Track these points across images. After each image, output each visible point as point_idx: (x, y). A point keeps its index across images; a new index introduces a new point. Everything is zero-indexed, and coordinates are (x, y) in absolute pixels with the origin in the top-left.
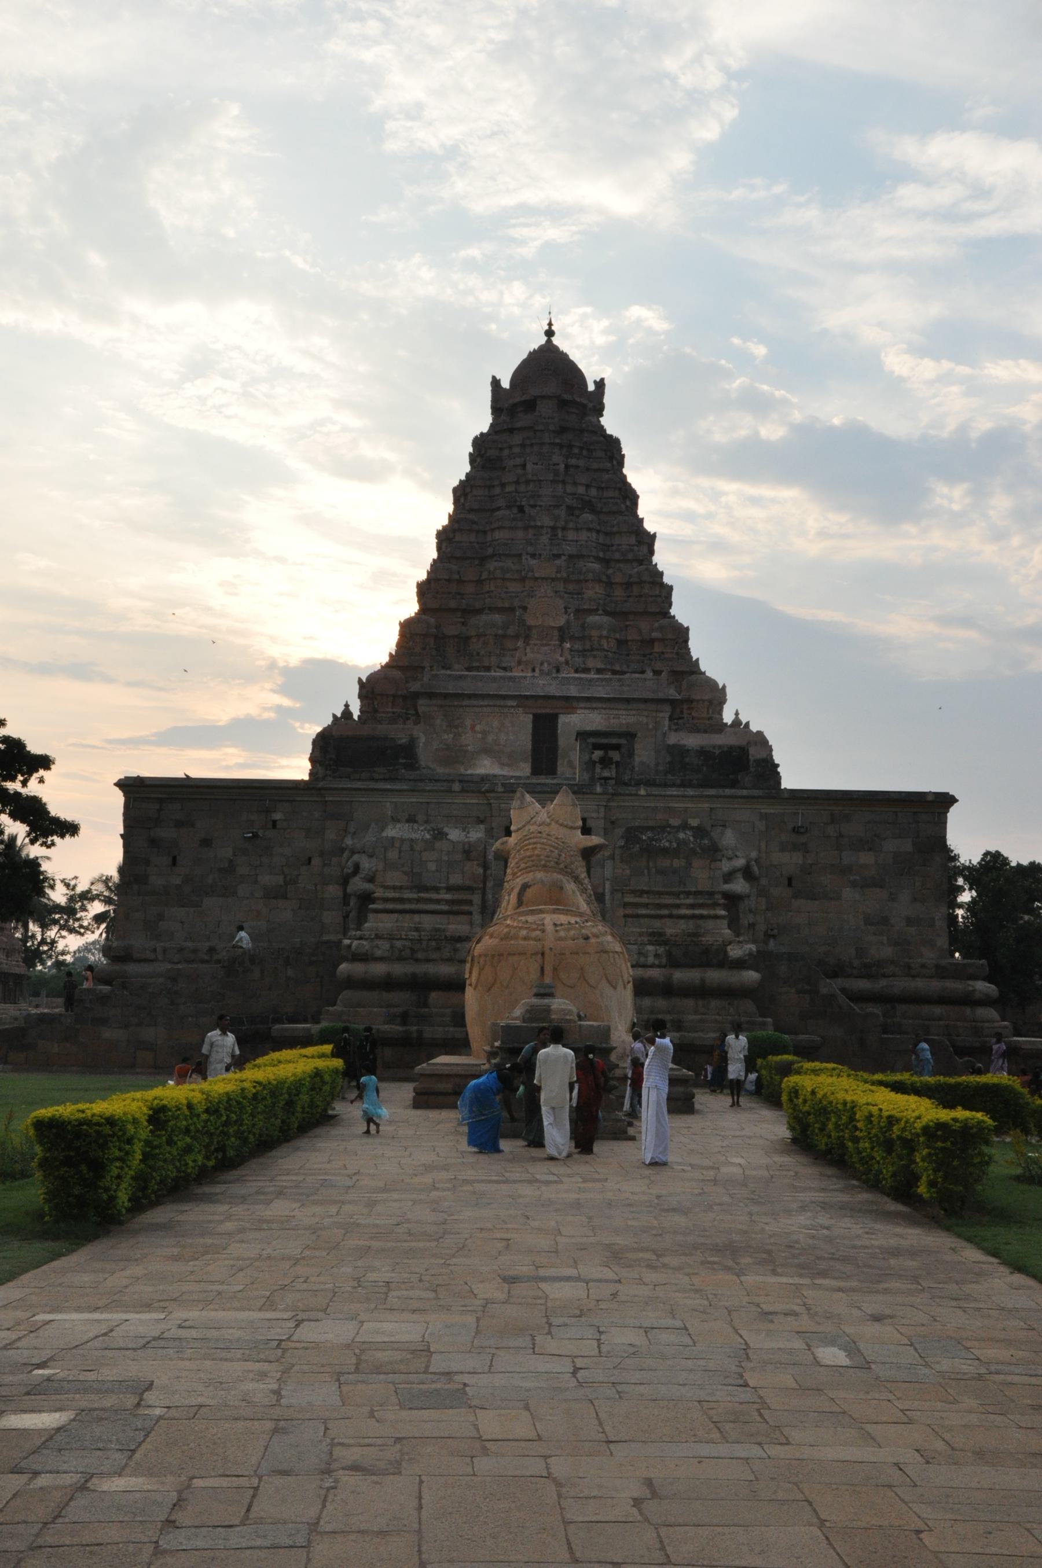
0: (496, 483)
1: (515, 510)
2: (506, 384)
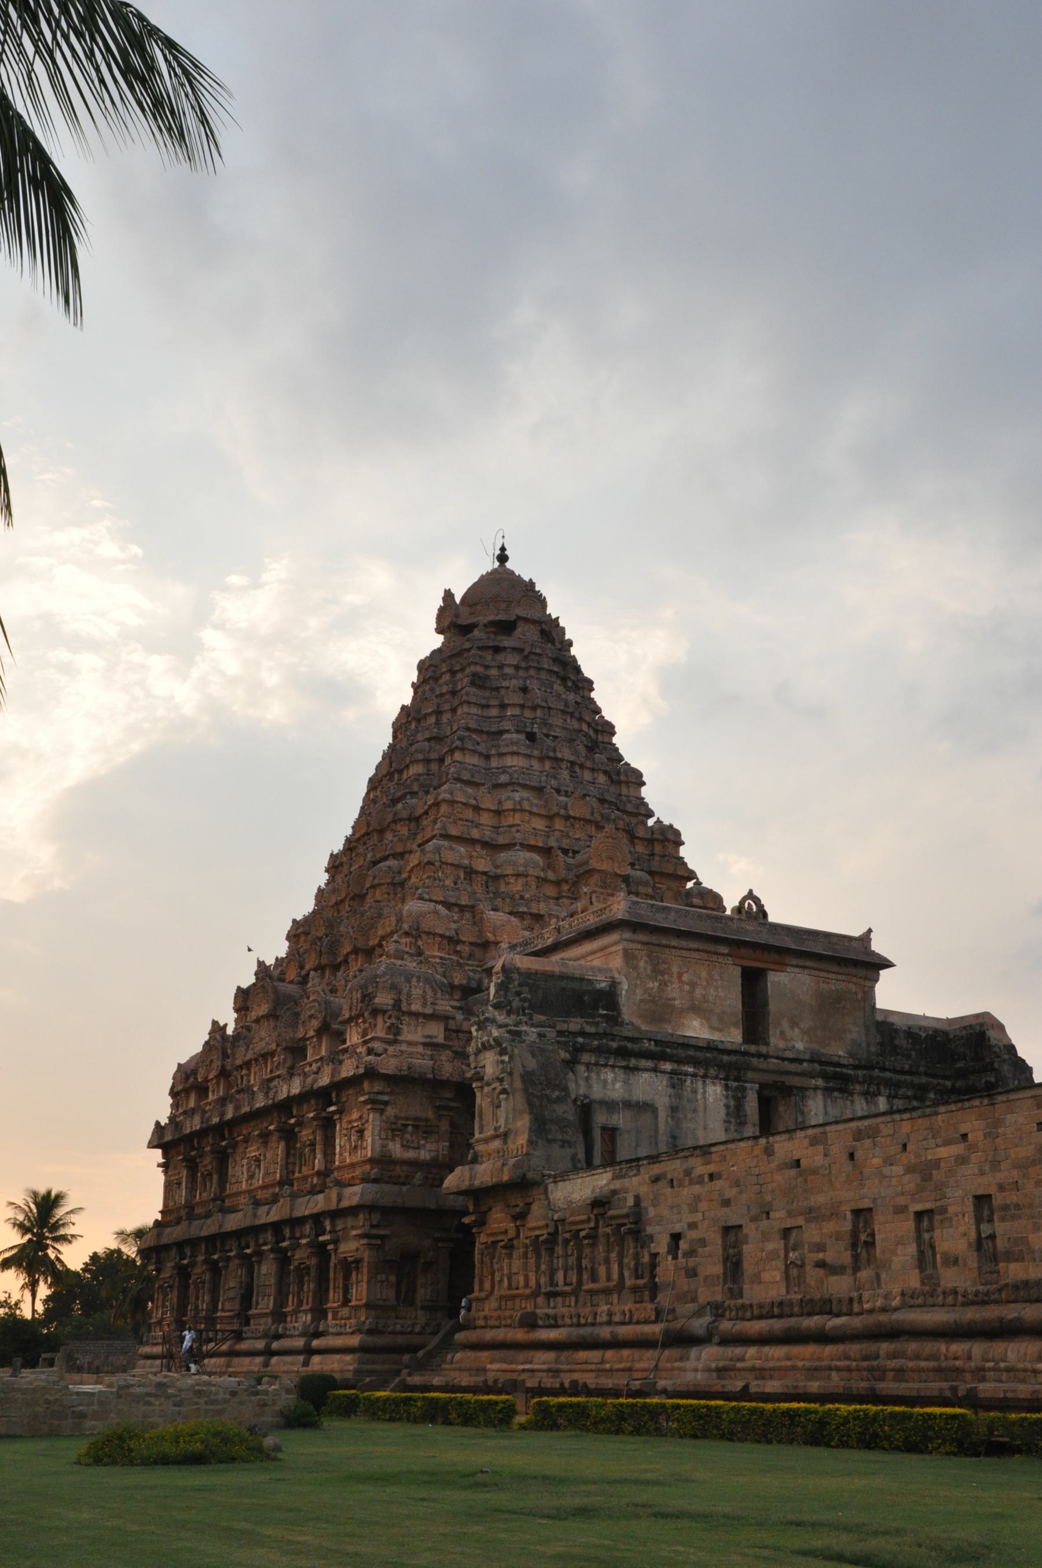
0: (494, 702)
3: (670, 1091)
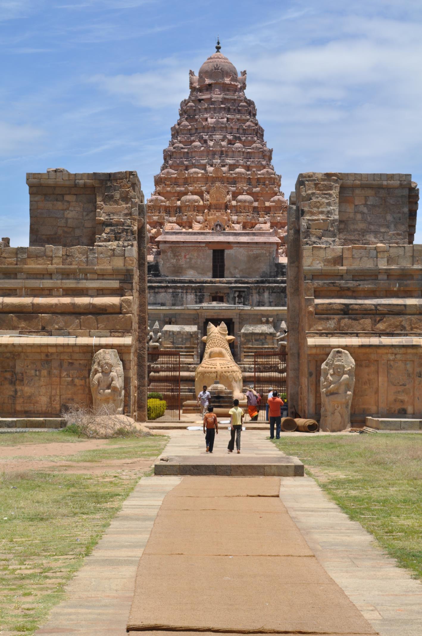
1: (203, 142)
2: (197, 74)
3: (173, 298)
